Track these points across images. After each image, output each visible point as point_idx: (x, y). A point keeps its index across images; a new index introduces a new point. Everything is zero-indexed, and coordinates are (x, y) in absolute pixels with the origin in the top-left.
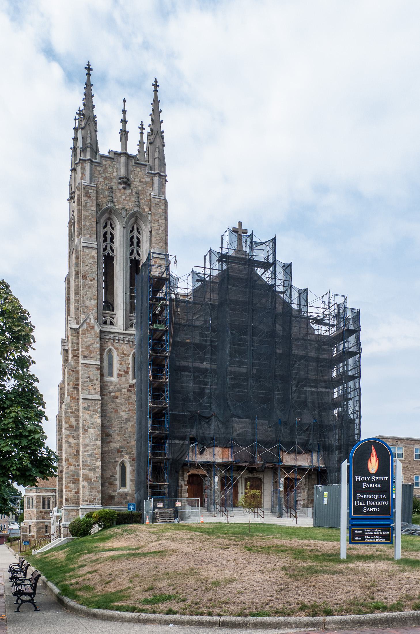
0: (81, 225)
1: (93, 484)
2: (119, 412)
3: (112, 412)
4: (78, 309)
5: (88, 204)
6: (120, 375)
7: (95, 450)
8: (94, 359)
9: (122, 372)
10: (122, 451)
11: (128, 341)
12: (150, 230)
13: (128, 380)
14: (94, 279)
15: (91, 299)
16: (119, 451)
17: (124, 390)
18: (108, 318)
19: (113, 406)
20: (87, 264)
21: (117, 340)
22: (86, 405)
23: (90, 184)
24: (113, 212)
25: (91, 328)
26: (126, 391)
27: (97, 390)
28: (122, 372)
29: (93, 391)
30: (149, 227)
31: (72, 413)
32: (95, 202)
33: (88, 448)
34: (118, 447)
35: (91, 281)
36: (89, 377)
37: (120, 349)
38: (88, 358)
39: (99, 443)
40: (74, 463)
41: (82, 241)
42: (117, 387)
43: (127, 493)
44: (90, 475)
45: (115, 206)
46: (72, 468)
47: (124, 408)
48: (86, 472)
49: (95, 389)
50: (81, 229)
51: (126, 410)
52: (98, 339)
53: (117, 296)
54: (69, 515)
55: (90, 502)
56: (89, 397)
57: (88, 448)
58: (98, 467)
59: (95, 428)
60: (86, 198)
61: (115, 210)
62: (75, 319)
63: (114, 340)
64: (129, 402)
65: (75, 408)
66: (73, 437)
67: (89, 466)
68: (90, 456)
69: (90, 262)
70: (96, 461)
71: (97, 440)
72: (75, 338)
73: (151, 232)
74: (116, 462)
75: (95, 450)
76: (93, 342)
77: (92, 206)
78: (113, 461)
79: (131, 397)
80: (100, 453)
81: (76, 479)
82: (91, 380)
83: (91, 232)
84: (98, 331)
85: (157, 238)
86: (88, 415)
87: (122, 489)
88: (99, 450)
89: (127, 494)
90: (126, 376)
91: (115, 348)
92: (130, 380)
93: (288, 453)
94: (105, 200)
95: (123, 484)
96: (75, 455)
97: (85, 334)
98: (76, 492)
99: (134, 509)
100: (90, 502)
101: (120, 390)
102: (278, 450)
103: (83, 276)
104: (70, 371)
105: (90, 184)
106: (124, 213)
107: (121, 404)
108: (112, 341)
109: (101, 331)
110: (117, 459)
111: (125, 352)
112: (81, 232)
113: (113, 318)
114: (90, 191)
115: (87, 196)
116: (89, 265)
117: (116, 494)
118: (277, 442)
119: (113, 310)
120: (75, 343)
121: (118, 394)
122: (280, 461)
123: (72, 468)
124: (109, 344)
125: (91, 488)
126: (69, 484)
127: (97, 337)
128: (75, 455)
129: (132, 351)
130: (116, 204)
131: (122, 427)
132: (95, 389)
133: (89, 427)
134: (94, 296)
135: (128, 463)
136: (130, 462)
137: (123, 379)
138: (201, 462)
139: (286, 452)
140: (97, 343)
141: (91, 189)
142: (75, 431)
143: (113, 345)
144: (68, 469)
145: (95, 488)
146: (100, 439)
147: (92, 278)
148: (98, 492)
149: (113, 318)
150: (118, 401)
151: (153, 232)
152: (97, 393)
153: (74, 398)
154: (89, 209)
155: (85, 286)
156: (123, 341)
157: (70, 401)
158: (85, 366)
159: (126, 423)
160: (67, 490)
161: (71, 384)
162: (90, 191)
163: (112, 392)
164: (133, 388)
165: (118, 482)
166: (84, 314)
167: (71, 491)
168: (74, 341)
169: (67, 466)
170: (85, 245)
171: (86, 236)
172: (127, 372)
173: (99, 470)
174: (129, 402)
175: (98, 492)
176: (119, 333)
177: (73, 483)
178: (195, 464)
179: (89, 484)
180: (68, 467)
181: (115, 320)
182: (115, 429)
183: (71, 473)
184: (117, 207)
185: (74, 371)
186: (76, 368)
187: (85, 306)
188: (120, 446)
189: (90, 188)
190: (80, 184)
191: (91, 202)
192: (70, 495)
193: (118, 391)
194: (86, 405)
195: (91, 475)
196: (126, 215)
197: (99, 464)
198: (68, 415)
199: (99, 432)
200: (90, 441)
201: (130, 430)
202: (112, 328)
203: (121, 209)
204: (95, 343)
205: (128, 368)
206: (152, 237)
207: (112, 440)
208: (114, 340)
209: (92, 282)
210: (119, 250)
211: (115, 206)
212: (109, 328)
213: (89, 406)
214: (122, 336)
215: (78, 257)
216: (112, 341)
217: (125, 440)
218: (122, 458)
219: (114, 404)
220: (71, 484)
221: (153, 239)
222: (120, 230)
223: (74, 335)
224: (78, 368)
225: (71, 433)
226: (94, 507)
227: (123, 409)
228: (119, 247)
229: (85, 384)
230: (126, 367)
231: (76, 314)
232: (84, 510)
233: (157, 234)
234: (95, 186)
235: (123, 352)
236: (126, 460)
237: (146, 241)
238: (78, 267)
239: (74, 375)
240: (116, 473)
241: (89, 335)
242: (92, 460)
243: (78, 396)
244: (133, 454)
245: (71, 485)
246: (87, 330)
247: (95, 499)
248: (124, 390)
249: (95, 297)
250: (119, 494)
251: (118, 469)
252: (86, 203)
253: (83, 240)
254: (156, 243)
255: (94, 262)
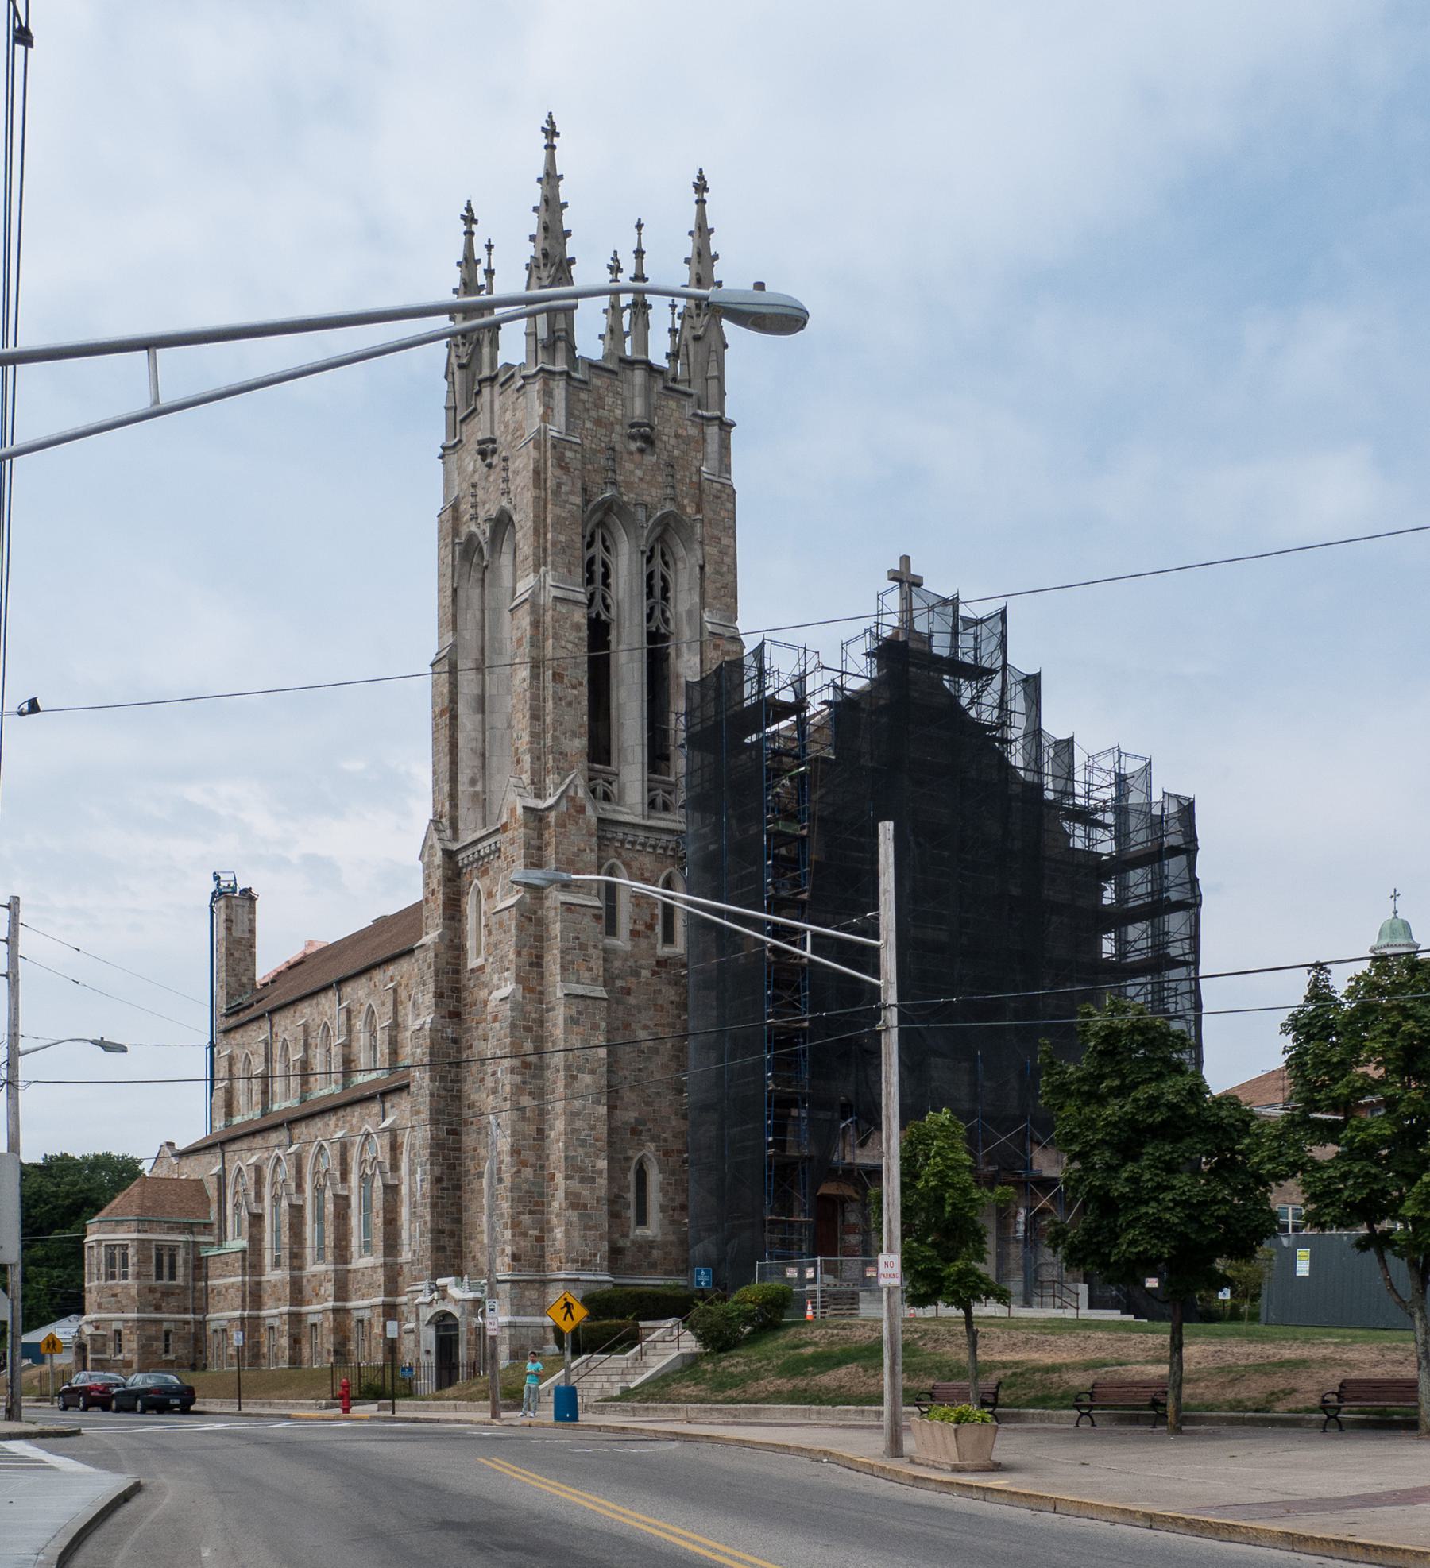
0: (545, 538)
1: (590, 1217)
2: (634, 1031)
3: (618, 1029)
4: (539, 759)
5: (564, 489)
6: (634, 934)
7: (593, 1128)
8: (585, 891)
9: (640, 927)
10: (641, 1131)
11: (654, 847)
12: (701, 562)
13: (654, 947)
14: (581, 684)
15: (574, 734)
16: (635, 1132)
17: (645, 973)
18: (598, 781)
19: (620, 1014)
20: (563, 643)
21: (629, 842)
22: (573, 1012)
23: (567, 434)
24: (615, 509)
25: (577, 812)
26: (649, 975)
27: (595, 972)
28: (640, 927)
29: (587, 974)
30: (699, 553)
31: (528, 1029)
32: (579, 484)
33: (579, 1124)
34: (633, 1120)
35: (574, 687)
36: (577, 938)
37: (635, 865)
38: (573, 889)
39: (602, 1110)
40: (532, 1160)
41: (549, 581)
42: (629, 964)
43: (653, 1242)
44: (584, 1193)
45: (621, 494)
46: (528, 1172)
47: (646, 1018)
48: (575, 1185)
49: (591, 970)
50: (545, 550)
51: (650, 1023)
52: (594, 840)
53: (621, 726)
54: (522, 1297)
55: (583, 1263)
56: (579, 990)
57: (579, 1124)
58: (600, 1172)
59: (593, 1072)
60: (558, 472)
61: (620, 507)
62: (533, 783)
63: (622, 842)
64: (655, 1005)
65: (533, 1015)
66: (530, 1094)
67: (581, 1170)
68: (583, 1143)
69: (571, 638)
70: (597, 1156)
71: (598, 1102)
72: (534, 834)
73: (702, 568)
74: (628, 1159)
75: (593, 1128)
76: (582, 846)
77: (572, 493)
78: (621, 1156)
79: (660, 991)
80: (604, 1136)
81: (537, 1204)
82: (583, 947)
83: (572, 559)
84: (594, 820)
85: (719, 585)
86: (579, 1037)
87: (639, 1232)
88: (602, 1129)
89: (651, 1244)
90: (648, 937)
91: (623, 863)
92: (659, 946)
93: (1045, 1147)
94: (598, 479)
95: (642, 1220)
96: (534, 1139)
97: (564, 826)
98: (536, 1237)
99: (707, 1283)
100: (584, 1264)
101: (635, 973)
102: (1024, 1141)
103: (554, 674)
104: (523, 919)
105: (567, 434)
106: (641, 514)
107: (639, 1008)
108: (617, 844)
109: (600, 820)
110: (630, 1153)
111: (647, 875)
112: (545, 557)
113: (669, 793)
114: (568, 454)
115: (561, 468)
116: (570, 646)
117: (629, 1244)
118: (1023, 1118)
119: (608, 763)
120: (533, 847)
121: (631, 982)
122: (1028, 1165)
123: (528, 1172)
124: (611, 852)
125: (587, 1228)
126: (522, 1217)
127: (591, 835)
128: (534, 1139)
129: (662, 871)
130: (623, 489)
131: (640, 1070)
132: (591, 970)
133: (580, 1070)
134: (581, 726)
135: (655, 1163)
136: (658, 1160)
137: (644, 943)
138: (866, 1165)
139: (1039, 1143)
140: (592, 850)
141: (571, 449)
142: (534, 1077)
143: (619, 856)
144: (519, 1177)
145: (595, 1227)
146: (604, 1100)
147: (574, 681)
148: (601, 1237)
149: (610, 783)
150: (632, 1000)
151: (708, 568)
152: (594, 980)
153: (531, 990)
154: (566, 501)
155: (561, 699)
156: (644, 845)
157: (524, 998)
158: (569, 910)
159: (649, 1059)
160: (518, 1230)
161: (524, 952)
162: (568, 454)
163: (618, 977)
164: (666, 967)
165: (631, 1213)
166: (559, 774)
167: (525, 1234)
168: (533, 842)
169: (515, 1169)
170: (559, 593)
171: (559, 569)
172: (651, 927)
173: (602, 1181)
174: (655, 1005)
175: (601, 1237)
176: (634, 826)
177: (531, 1212)
178: (853, 1171)
179: (581, 1217)
180: (519, 1171)
181: (614, 788)
182: (627, 1073)
183: (525, 1186)
184: (625, 498)
185: (530, 919)
186: (535, 912)
187: (561, 753)
188: (636, 1119)
189: (568, 445)
190: (542, 433)
191: (570, 483)
192: (522, 1244)
193: (632, 975)
194: (573, 1012)
195: (586, 1193)
196: (647, 521)
197: (602, 1164)
198: (517, 1034)
199: (604, 1082)
200: (584, 1106)
201: (658, 1077)
202: (614, 811)
203: (635, 505)
204: (588, 851)
205: (653, 916)
206: (707, 583)
207: (619, 1103)
208: (622, 842)
209: (575, 692)
210: (626, 607)
211: (621, 494)
212: (611, 812)
213: (579, 1013)
214: (641, 833)
215: (539, 622)
216: (617, 844)
217: (647, 1104)
218: (641, 1150)
219: (621, 1007)
220: (527, 1217)
221: (710, 587)
222: (630, 560)
223: (532, 825)
224: (540, 912)
225: (524, 1083)
226: (592, 1278)
227: (643, 1022)
228: (627, 599)
229: (569, 957)
230: (648, 912)
231: (534, 772)
232: (571, 1285)
233: (717, 572)
234: (578, 441)
235: (643, 875)
236: (649, 1154)
237: (690, 589)
238: (538, 647)
239: (532, 930)
240: (628, 1187)
241: (572, 828)
242: (587, 1155)
243: (541, 985)
244: (665, 1140)
245: (526, 1219)
246: (570, 816)
247: (595, 1255)
248: (645, 973)
249: (582, 730)
250: (633, 1242)
251: (631, 1177)
252: (559, 485)
253: (554, 580)
254: (715, 598)
255: (580, 639)
